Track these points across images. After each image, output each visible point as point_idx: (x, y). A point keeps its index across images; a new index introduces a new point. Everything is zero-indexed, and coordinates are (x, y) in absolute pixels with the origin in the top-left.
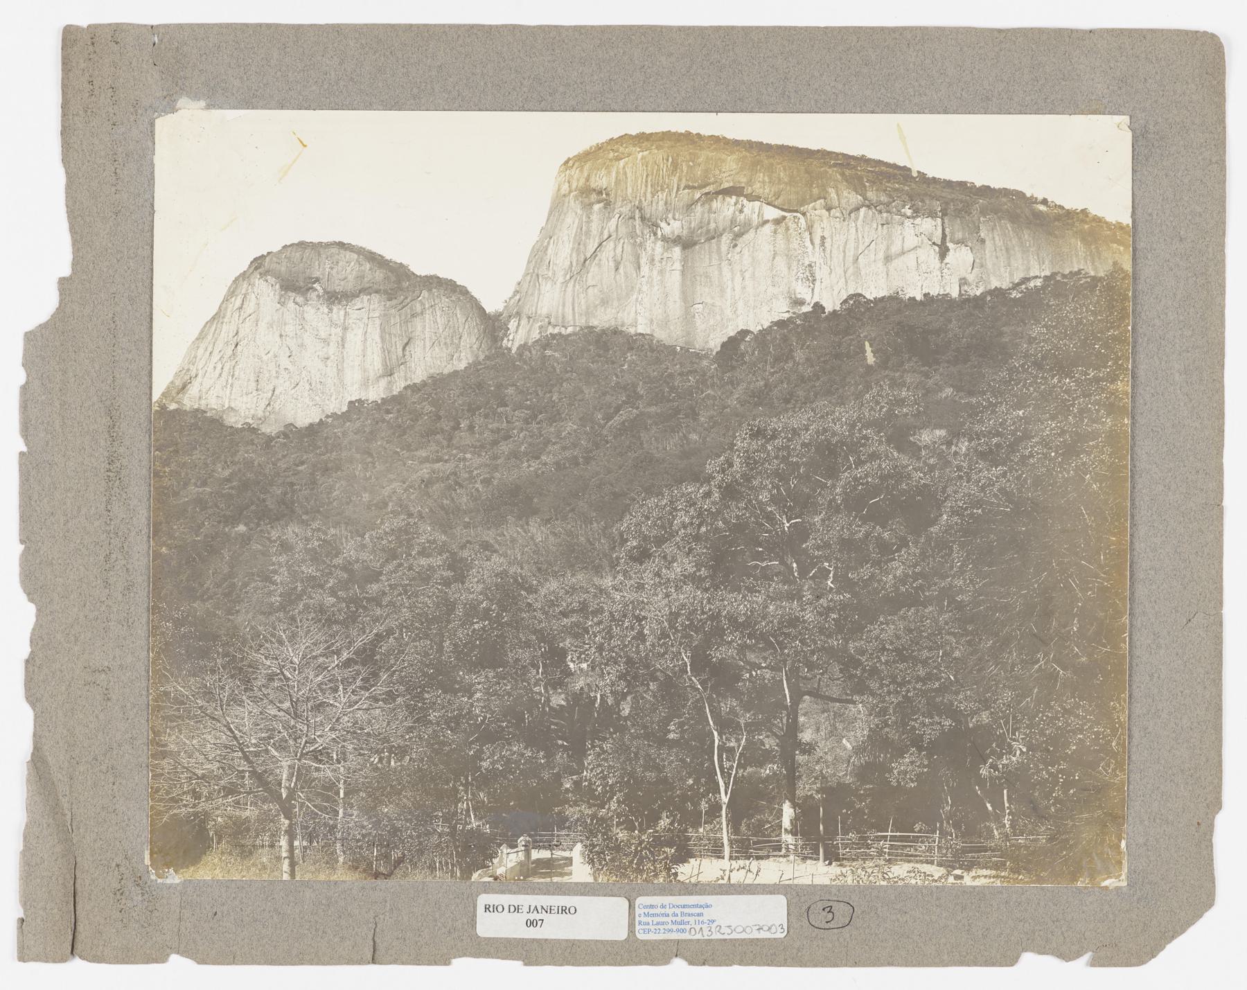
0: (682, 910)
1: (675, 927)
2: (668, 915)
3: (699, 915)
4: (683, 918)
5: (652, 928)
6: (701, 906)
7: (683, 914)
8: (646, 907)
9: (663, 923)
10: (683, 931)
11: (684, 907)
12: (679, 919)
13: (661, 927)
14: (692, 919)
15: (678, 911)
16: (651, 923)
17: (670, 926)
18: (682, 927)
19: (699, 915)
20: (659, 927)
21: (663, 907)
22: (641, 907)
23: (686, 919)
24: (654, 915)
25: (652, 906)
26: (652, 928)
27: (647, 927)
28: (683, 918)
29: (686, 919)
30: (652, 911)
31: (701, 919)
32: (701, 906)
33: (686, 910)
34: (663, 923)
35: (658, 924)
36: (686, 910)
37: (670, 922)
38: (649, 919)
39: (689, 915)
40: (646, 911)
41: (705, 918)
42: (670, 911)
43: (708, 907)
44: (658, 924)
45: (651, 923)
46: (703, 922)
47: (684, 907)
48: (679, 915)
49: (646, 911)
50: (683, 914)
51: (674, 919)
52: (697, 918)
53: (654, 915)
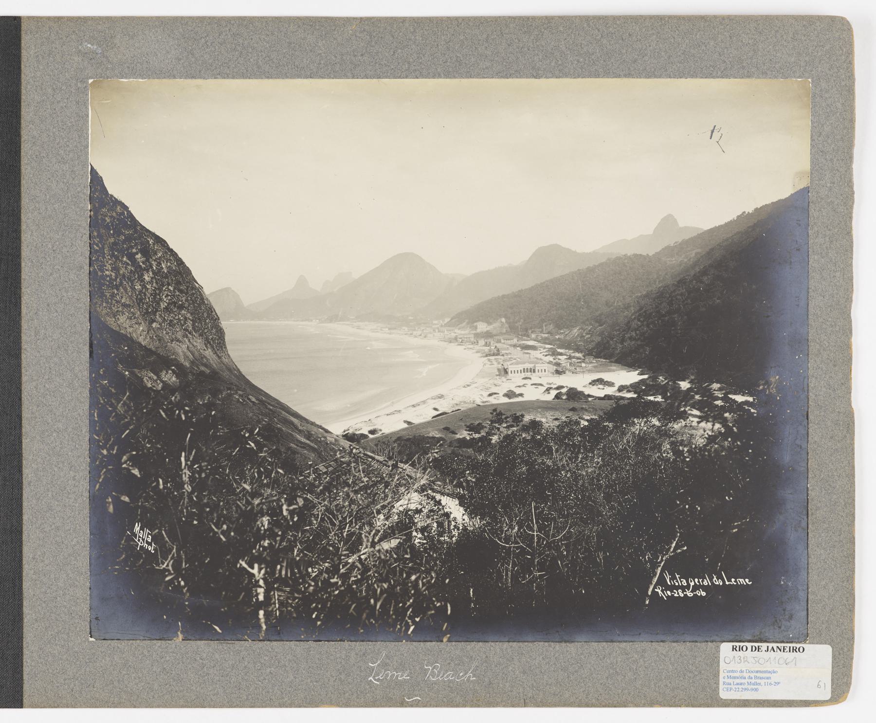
0: (756, 674)
1: (750, 687)
2: (745, 678)
3: (768, 678)
4: (756, 681)
5: (732, 686)
6: (770, 672)
7: (756, 677)
8: (729, 672)
9: (741, 684)
10: (756, 690)
11: (757, 672)
12: (753, 681)
13: (740, 687)
14: (762, 682)
15: (752, 675)
16: (732, 684)
17: (746, 686)
18: (756, 687)
19: (768, 678)
20: (737, 687)
21: (742, 672)
22: (725, 671)
23: (758, 681)
24: (734, 678)
25: (733, 671)
26: (732, 686)
27: (729, 686)
28: (756, 681)
29: (758, 681)
30: (732, 675)
31: (769, 681)
32: (770, 672)
33: (758, 675)
34: (741, 684)
35: (737, 684)
36: (758, 675)
37: (746, 683)
38: (731, 681)
39: (761, 679)
40: (729, 674)
41: (772, 681)
42: (745, 675)
43: (774, 672)
44: (737, 684)
45: (732, 684)
46: (771, 684)
47: (757, 672)
48: (753, 678)
49: (729, 674)
50: (756, 677)
51: (750, 681)
52: (768, 680)
53: (734, 678)
